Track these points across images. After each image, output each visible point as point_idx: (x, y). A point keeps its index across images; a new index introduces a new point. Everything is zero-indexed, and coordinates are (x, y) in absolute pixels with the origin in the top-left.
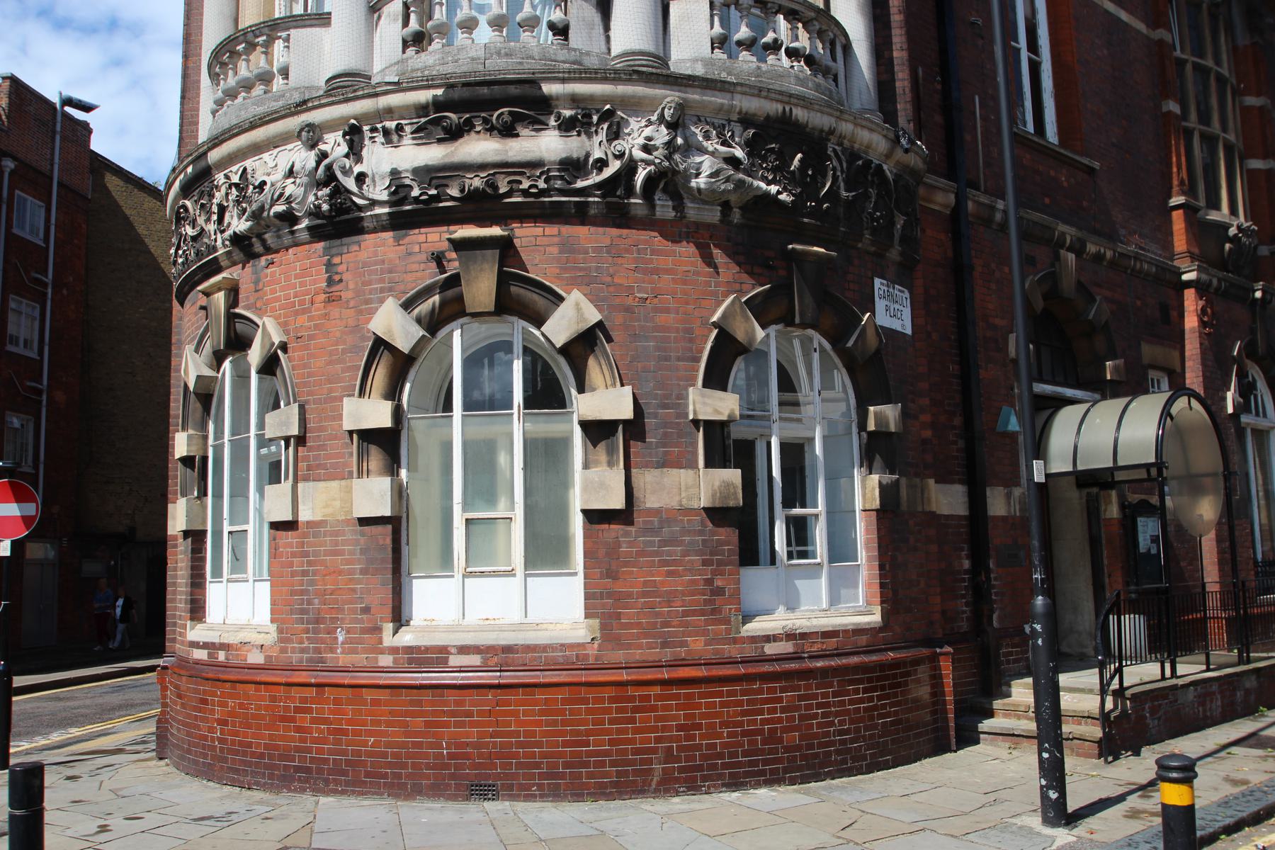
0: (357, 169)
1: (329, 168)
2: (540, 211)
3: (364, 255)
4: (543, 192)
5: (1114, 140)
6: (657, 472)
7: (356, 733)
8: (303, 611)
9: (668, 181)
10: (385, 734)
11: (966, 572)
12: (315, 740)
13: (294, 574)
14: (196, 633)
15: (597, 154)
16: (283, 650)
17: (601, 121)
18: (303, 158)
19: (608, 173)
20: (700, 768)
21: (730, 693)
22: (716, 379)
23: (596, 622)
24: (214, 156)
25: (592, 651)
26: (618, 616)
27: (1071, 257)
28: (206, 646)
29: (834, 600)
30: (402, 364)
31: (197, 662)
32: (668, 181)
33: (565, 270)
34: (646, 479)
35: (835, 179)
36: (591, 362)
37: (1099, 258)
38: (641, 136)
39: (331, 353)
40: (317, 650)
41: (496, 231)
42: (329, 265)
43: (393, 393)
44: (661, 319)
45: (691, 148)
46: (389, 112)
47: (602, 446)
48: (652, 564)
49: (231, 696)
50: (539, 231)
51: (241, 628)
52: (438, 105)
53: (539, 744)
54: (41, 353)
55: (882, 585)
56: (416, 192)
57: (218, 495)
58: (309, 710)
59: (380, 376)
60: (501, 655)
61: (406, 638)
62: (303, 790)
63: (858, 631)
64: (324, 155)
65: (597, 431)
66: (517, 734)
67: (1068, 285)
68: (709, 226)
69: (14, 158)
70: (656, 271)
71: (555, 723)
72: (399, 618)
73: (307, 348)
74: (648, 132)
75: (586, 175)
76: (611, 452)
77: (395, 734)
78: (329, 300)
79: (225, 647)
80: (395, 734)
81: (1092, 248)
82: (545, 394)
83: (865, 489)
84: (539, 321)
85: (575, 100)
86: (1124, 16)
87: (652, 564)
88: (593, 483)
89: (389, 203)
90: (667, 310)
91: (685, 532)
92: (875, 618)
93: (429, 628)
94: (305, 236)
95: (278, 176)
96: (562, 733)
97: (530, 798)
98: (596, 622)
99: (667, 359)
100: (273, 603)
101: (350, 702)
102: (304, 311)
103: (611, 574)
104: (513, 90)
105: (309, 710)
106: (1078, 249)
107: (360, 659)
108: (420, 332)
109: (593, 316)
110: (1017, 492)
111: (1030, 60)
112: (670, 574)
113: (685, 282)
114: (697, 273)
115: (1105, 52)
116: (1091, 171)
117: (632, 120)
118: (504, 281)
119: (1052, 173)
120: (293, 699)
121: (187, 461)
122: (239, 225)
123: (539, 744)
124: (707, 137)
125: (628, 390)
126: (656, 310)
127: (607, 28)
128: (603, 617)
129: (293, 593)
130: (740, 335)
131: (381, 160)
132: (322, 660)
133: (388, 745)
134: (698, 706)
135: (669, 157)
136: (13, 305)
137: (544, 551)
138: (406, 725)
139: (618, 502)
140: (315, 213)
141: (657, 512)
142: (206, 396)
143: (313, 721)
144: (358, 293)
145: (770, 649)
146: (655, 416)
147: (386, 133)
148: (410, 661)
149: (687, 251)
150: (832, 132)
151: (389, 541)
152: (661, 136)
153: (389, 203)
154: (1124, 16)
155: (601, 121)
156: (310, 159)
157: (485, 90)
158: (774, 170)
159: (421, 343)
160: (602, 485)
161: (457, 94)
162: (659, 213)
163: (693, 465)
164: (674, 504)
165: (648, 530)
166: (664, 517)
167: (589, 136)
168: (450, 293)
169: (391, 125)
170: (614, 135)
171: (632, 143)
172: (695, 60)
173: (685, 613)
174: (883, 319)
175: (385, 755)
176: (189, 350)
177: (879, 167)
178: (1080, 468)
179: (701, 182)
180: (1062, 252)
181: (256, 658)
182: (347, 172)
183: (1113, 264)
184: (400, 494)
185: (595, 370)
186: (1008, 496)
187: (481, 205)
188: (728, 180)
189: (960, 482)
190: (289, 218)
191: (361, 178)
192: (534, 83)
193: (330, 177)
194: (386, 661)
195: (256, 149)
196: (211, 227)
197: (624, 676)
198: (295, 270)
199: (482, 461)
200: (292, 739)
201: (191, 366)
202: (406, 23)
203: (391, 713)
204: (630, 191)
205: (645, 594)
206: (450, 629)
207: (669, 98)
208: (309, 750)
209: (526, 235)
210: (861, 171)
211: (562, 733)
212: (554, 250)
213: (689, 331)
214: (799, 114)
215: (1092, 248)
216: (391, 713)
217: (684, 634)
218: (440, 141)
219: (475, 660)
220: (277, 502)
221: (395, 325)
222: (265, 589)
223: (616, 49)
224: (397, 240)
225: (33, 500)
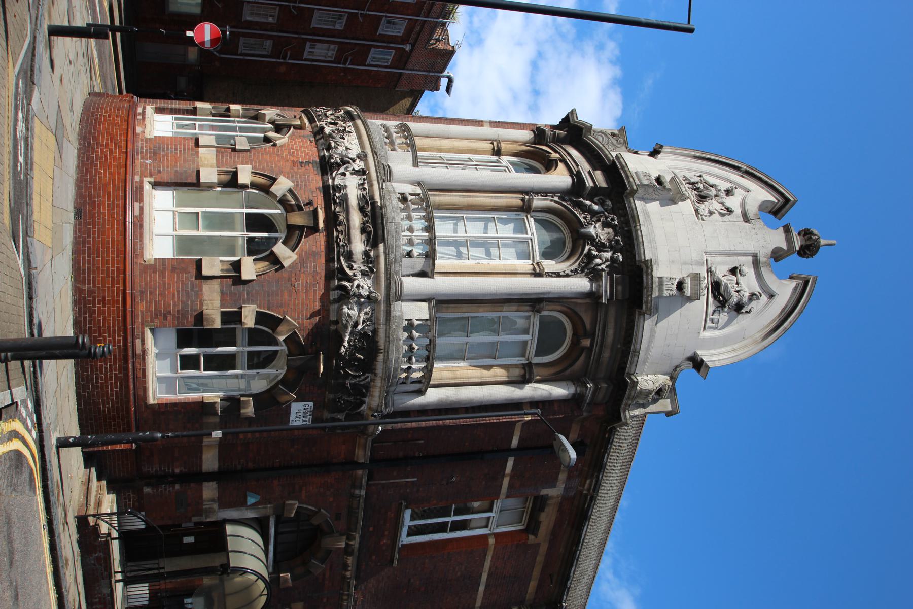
0: (348, 173)
1: (349, 162)
2: (330, 243)
3: (312, 175)
4: (338, 244)
5: (412, 580)
6: (219, 290)
7: (105, 166)
8: (159, 148)
9: (345, 296)
10: (105, 176)
11: (173, 470)
12: (102, 150)
13: (176, 145)
14: (149, 109)
15: (355, 266)
16: (142, 140)
17: (370, 268)
18: (353, 154)
19: (347, 270)
20: (85, 306)
21: (118, 321)
22: (261, 317)
23: (152, 262)
24: (359, 122)
25: (140, 261)
26: (155, 272)
27: (342, 545)
28: (144, 113)
29: (161, 380)
30: (265, 189)
31: (136, 109)
32: (345, 296)
33: (306, 253)
35: (355, 377)
36: (267, 263)
37: (345, 567)
38: (365, 285)
39: (271, 163)
40: (142, 153)
41: (321, 225)
42: (309, 163)
43: (254, 185)
44: (286, 294)
45: (361, 306)
46: (371, 185)
47: (230, 267)
48: (178, 287)
49: (122, 120)
50: (322, 243)
51: (152, 126)
52: (374, 204)
53: (99, 237)
54: (306, 60)
55: (167, 404)
56: (337, 195)
57: (212, 121)
58: (115, 148)
59: (261, 180)
60: (139, 223)
61: (147, 187)
62: (80, 144)
63: (145, 390)
64: (354, 161)
65: (237, 266)
66: (103, 228)
67: (328, 542)
68: (328, 315)
69: (412, 51)
70: (307, 291)
71: (108, 243)
72: (156, 185)
73: (274, 153)
74: (365, 287)
75: (346, 261)
76: (227, 271)
77: (105, 180)
78: (294, 162)
79: (144, 119)
80: (105, 180)
81: (350, 560)
82: (253, 247)
83: (213, 397)
84: (284, 243)
85: (377, 257)
86: (482, 588)
87: (178, 287)
88: (213, 266)
89: (333, 185)
90: (290, 296)
91: (192, 302)
92: (151, 401)
93: (151, 196)
94: (322, 154)
95: (347, 144)
96: (103, 247)
97: (75, 232)
98: (152, 262)
99: (269, 296)
100: (163, 137)
101: (119, 164)
102: (290, 153)
103: (174, 269)
104: (380, 232)
105: (115, 148)
107: (138, 169)
108: (279, 195)
109: (286, 264)
110: (215, 506)
111: (451, 530)
112: (174, 295)
113: (303, 304)
114: (307, 309)
115: (459, 574)
116: (392, 562)
117: (370, 281)
118: (301, 228)
119: (386, 533)
120: (120, 142)
121: (228, 109)
122: (327, 130)
123: (99, 237)
124: (366, 314)
125: (255, 278)
126: (290, 291)
127: (414, 275)
128: (155, 265)
129: (168, 145)
130: (280, 329)
132: (137, 154)
133: (100, 178)
134: (113, 306)
135: (354, 295)
136: (332, 46)
137: (183, 243)
138: (109, 184)
139: (205, 272)
140: (330, 157)
141: (201, 290)
142: (257, 118)
143: (111, 150)
144: (296, 173)
145: (138, 342)
146: (244, 290)
147: (363, 184)
148: (137, 188)
149: (317, 305)
150: (375, 375)
151: (189, 181)
152: (364, 292)
153: (333, 185)
154: (482, 588)
155: (370, 268)
157: (380, 221)
158: (355, 345)
159: (275, 196)
160: (213, 266)
161: (378, 211)
162: (332, 293)
163: (222, 306)
164: (205, 298)
165: (193, 286)
166: (199, 293)
167: (363, 263)
168: (296, 208)
169: (366, 186)
170: (364, 274)
171: (360, 280)
172: (401, 312)
173: (155, 302)
174: (296, 407)
175: (96, 176)
176: (278, 111)
177: (364, 403)
178: (228, 538)
179: (346, 310)
180: (345, 537)
181: (139, 130)
182: (346, 169)
183: (344, 577)
184: (210, 186)
185: (263, 265)
186: (213, 500)
187: (332, 220)
188: (347, 321)
189: (219, 467)
190: (329, 148)
191: (344, 174)
192: (383, 240)
193: (344, 163)
194: (137, 178)
195: (359, 137)
196: (329, 120)
197: (128, 274)
198: (308, 150)
199: (225, 221)
200: (103, 141)
201: (270, 112)
202: (411, 194)
203: (114, 179)
204: (340, 280)
205: (165, 284)
206: (150, 204)
207: (381, 296)
208: (98, 147)
209: (321, 238)
210: (361, 391)
211: (103, 247)
212: (314, 249)
213: (281, 306)
214: (381, 357)
215: (350, 560)
216: (114, 179)
217: (146, 301)
218: (359, 204)
219: (137, 213)
220: (207, 138)
221: (282, 186)
222: (170, 135)
224: (319, 188)
225: (212, 46)
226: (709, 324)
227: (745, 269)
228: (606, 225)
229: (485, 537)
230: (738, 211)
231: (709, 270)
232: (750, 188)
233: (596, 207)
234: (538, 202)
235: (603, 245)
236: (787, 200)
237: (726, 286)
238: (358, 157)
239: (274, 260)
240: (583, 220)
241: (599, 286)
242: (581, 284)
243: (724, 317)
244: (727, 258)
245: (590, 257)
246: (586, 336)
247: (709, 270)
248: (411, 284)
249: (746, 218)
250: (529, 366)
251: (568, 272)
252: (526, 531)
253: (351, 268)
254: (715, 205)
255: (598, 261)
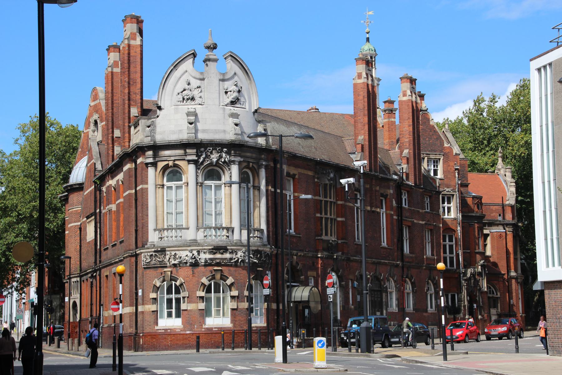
2: (226, 265)
3: (199, 270)
18: (190, 255)
27: (295, 257)
32: (243, 261)
34: (239, 304)
37: (301, 255)
41: (220, 268)
42: (193, 271)
44: (241, 281)
46: (205, 249)
52: (212, 249)
59: (202, 288)
61: (206, 327)
63: (264, 327)
64: (193, 255)
65: (233, 297)
67: (294, 263)
81: (299, 254)
84: (225, 281)
85: (231, 249)
92: (265, 325)
93: (209, 325)
103: (235, 317)
106: (296, 255)
107: (199, 329)
109: (233, 281)
118: (221, 275)
131: (204, 257)
140: (192, 263)
152: (243, 255)
156: (191, 255)
166: (242, 309)
170: (236, 254)
171: (239, 256)
183: (303, 256)
185: (233, 288)
187: (218, 264)
190: (186, 263)
191: (200, 259)
192: (226, 247)
193: (195, 258)
194: (203, 330)
214: (259, 249)
223: (235, 239)
226: (244, 107)
227: (226, 87)
228: (211, 153)
229: (294, 196)
230: (198, 83)
231: (226, 105)
232: (185, 70)
233: (204, 156)
234: (200, 180)
235: (220, 156)
236: (193, 54)
237: (233, 98)
238: (191, 252)
239: (232, 284)
240: (208, 162)
241: (237, 161)
242: (235, 169)
243: (242, 99)
244: (221, 96)
245: (225, 162)
246: (249, 165)
247: (226, 105)
248: (236, 236)
249: (203, 79)
250: (254, 187)
251: (229, 172)
252: (294, 179)
253: (235, 259)
254: (196, 93)
255: (226, 159)
